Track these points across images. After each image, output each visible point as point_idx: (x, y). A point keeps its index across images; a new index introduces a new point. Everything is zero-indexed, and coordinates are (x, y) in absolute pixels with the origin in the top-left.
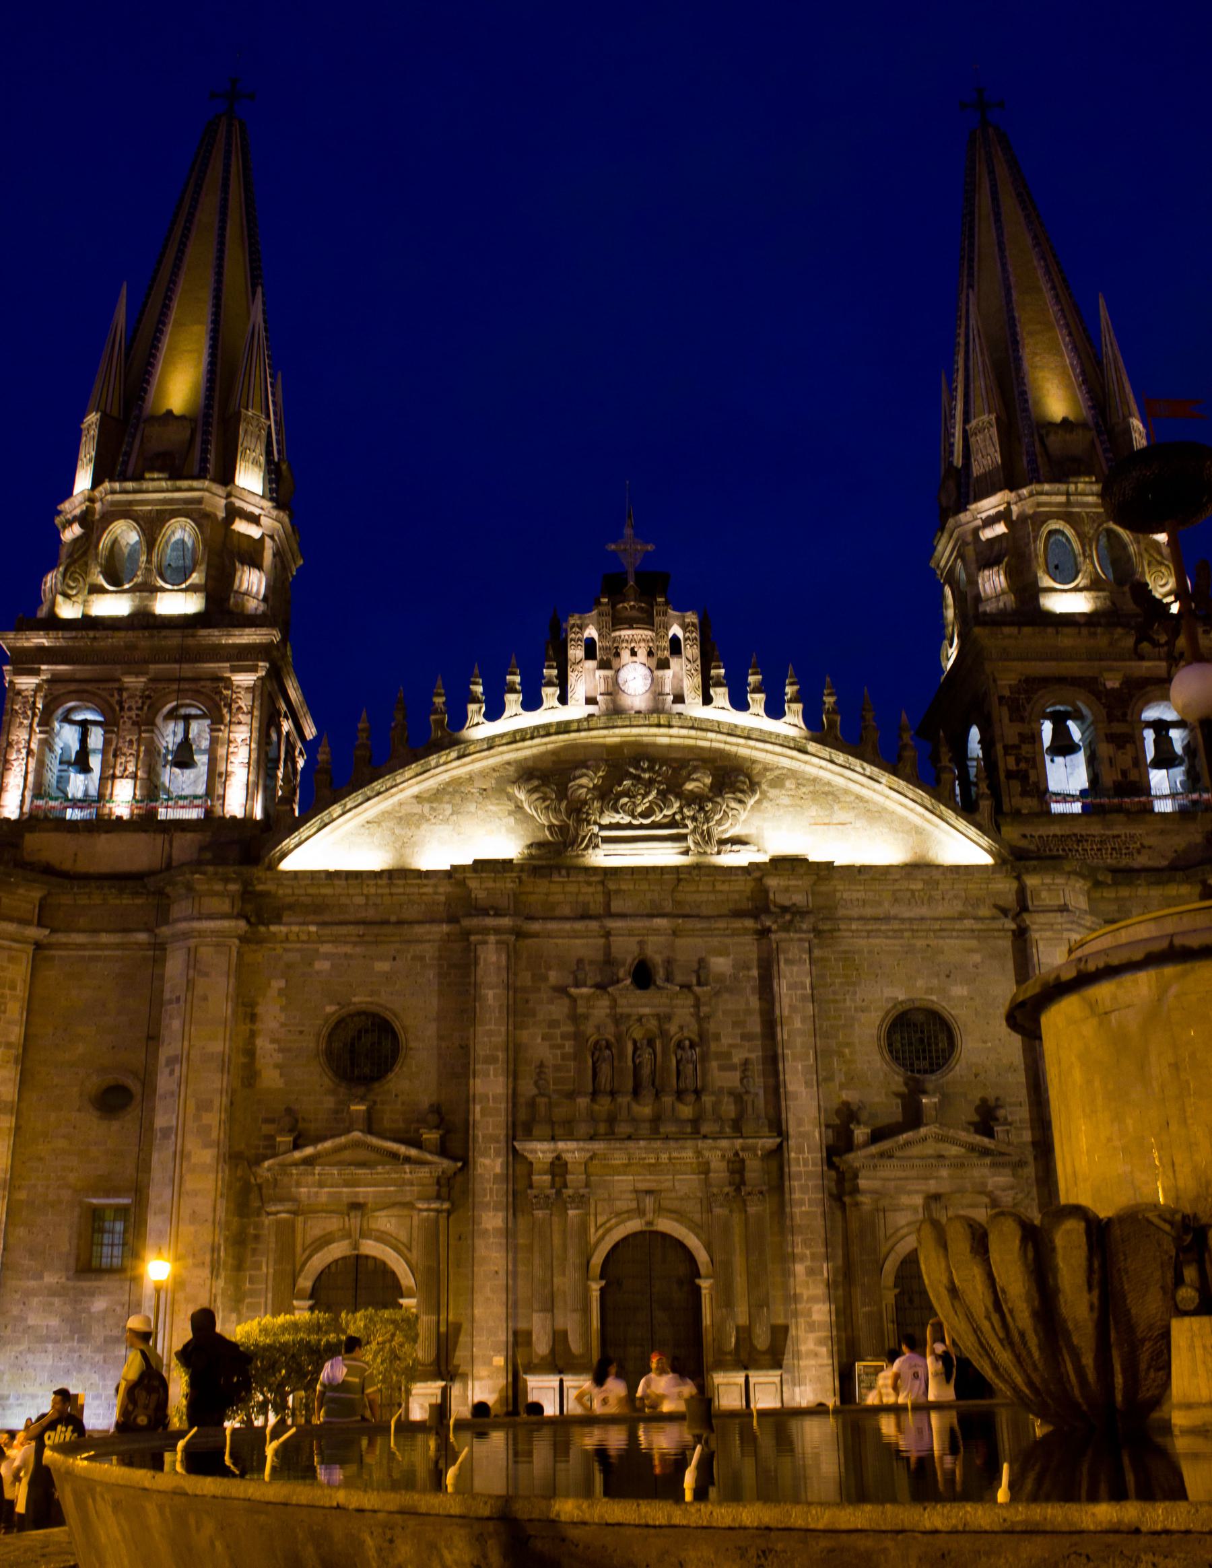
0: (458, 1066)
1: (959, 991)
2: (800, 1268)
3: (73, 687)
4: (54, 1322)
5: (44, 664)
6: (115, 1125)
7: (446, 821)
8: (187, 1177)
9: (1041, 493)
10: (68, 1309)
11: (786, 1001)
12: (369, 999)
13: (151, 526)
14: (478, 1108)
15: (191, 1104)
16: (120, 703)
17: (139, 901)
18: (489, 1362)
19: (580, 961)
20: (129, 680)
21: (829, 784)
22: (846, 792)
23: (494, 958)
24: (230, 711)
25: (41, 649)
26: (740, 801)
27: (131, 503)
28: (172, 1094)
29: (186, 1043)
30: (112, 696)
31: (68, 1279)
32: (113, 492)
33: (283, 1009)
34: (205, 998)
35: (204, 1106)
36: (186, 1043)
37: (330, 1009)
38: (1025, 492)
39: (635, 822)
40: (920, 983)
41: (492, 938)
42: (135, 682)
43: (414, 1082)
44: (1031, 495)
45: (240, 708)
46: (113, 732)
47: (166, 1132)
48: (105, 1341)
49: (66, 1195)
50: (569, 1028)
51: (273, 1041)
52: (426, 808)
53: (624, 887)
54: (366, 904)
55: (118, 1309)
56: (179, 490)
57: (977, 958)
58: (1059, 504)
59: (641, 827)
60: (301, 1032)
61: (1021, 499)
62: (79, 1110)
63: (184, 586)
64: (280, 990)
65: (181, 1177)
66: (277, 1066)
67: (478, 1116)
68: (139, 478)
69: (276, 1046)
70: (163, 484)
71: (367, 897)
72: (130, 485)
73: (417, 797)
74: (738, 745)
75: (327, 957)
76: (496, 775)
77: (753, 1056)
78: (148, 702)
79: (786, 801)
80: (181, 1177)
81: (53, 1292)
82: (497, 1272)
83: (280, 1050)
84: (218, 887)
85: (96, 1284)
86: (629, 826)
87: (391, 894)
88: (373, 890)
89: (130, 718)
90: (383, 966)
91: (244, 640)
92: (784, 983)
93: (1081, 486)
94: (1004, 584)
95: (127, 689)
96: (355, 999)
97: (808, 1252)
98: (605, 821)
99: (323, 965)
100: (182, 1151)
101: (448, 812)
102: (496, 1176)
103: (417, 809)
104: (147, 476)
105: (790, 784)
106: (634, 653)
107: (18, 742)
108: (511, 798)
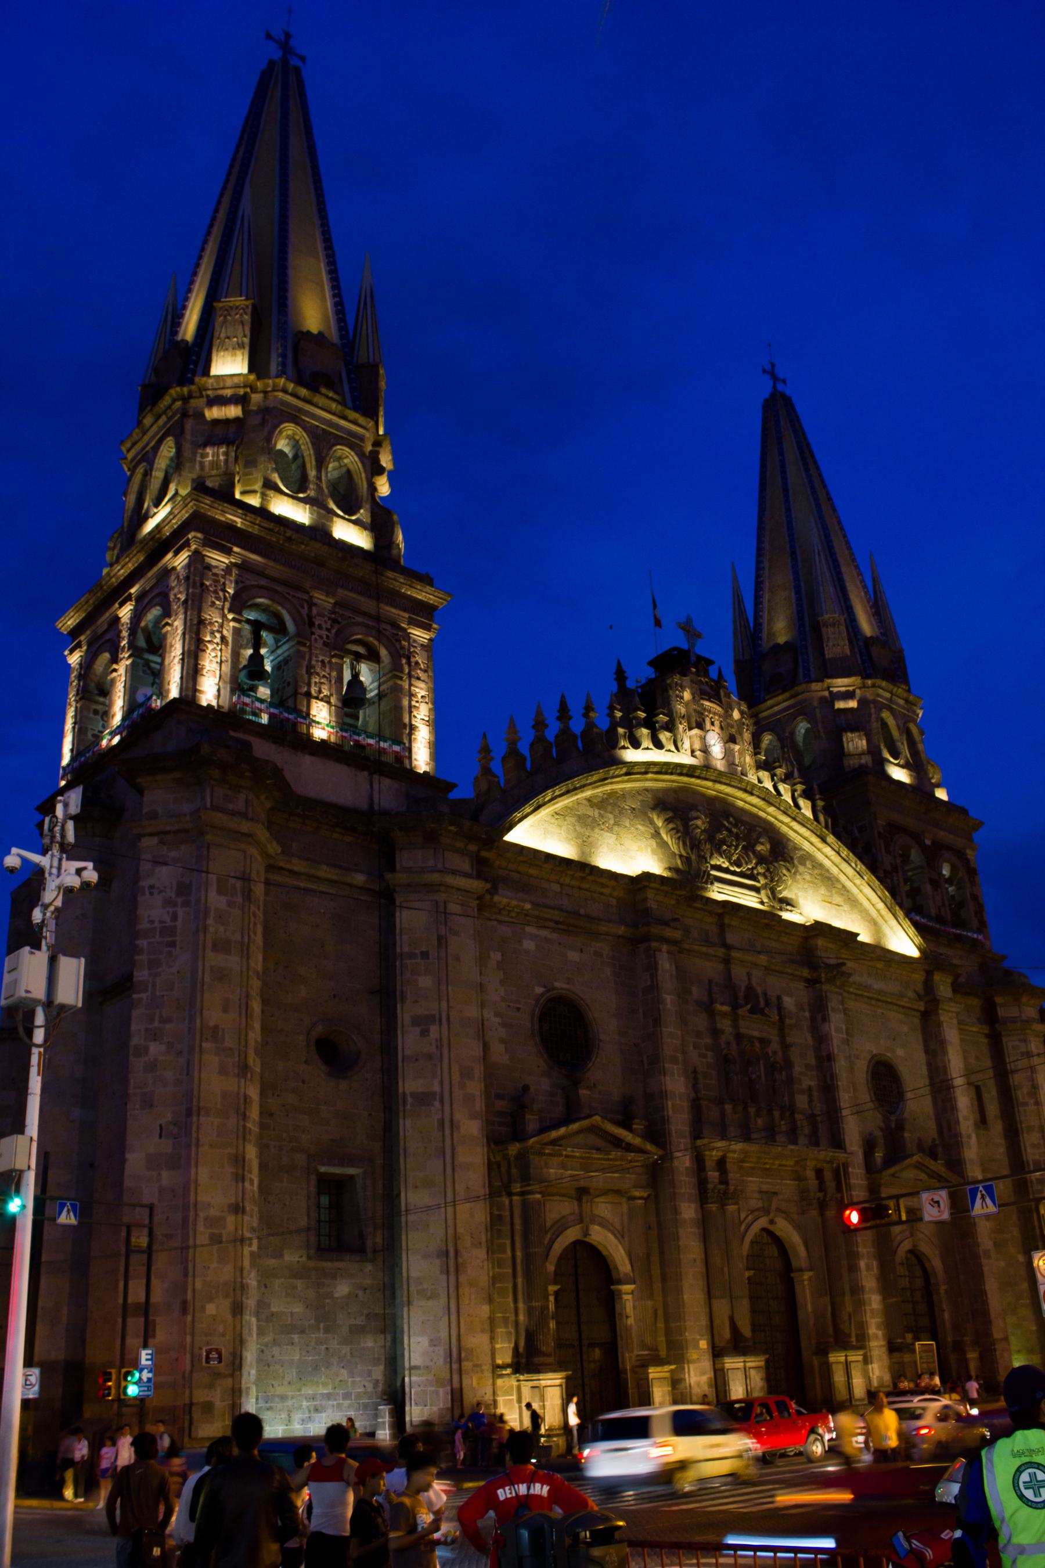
0: (645, 1062)
1: (900, 1052)
2: (862, 1264)
3: (263, 582)
4: (298, 1309)
5: (238, 546)
6: (343, 1085)
7: (610, 830)
8: (459, 1149)
9: (880, 687)
10: (311, 1294)
11: (835, 1042)
12: (566, 986)
13: (323, 442)
14: (670, 1103)
15: (455, 1069)
16: (310, 617)
17: (348, 839)
18: (697, 1347)
19: (710, 982)
20: (319, 596)
21: (828, 871)
22: (838, 880)
23: (667, 966)
24: (409, 663)
25: (231, 527)
26: (789, 870)
27: (300, 410)
28: (429, 1057)
29: (444, 1004)
30: (303, 607)
31: (309, 1258)
32: (285, 391)
33: (502, 982)
34: (457, 958)
35: (466, 1074)
36: (444, 1004)
37: (539, 990)
38: (869, 682)
39: (732, 868)
40: (882, 1042)
41: (665, 947)
42: (324, 600)
43: (606, 1075)
44: (874, 686)
45: (417, 663)
46: (304, 645)
47: (424, 1099)
48: (351, 1331)
49: (301, 1159)
50: (709, 1041)
51: (497, 1014)
52: (596, 813)
53: (733, 923)
54: (561, 893)
55: (360, 1293)
56: (345, 418)
57: (905, 1029)
58: (886, 699)
59: (734, 873)
60: (518, 1009)
61: (864, 686)
62: (306, 1062)
63: (354, 518)
64: (498, 962)
65: (453, 1149)
66: (502, 1041)
67: (670, 1112)
68: (314, 389)
69: (498, 1020)
70: (334, 406)
71: (562, 885)
72: (303, 392)
73: (589, 800)
74: (782, 822)
75: (533, 937)
76: (640, 798)
77: (813, 1083)
78: (336, 627)
79: (808, 877)
80: (453, 1149)
81: (295, 1274)
82: (695, 1260)
83: (504, 1025)
84: (459, 844)
85: (340, 1265)
86: (726, 871)
87: (580, 888)
88: (567, 880)
89: (321, 637)
90: (574, 956)
91: (420, 596)
92: (832, 1026)
93: (900, 690)
94: (865, 748)
95: (315, 605)
96: (557, 984)
97: (865, 1251)
98: (713, 862)
99: (529, 945)
100: (452, 1121)
101: (612, 822)
102: (687, 1168)
103: (590, 812)
104: (323, 390)
105: (808, 864)
106: (712, 724)
107: (211, 624)
108: (652, 822)
